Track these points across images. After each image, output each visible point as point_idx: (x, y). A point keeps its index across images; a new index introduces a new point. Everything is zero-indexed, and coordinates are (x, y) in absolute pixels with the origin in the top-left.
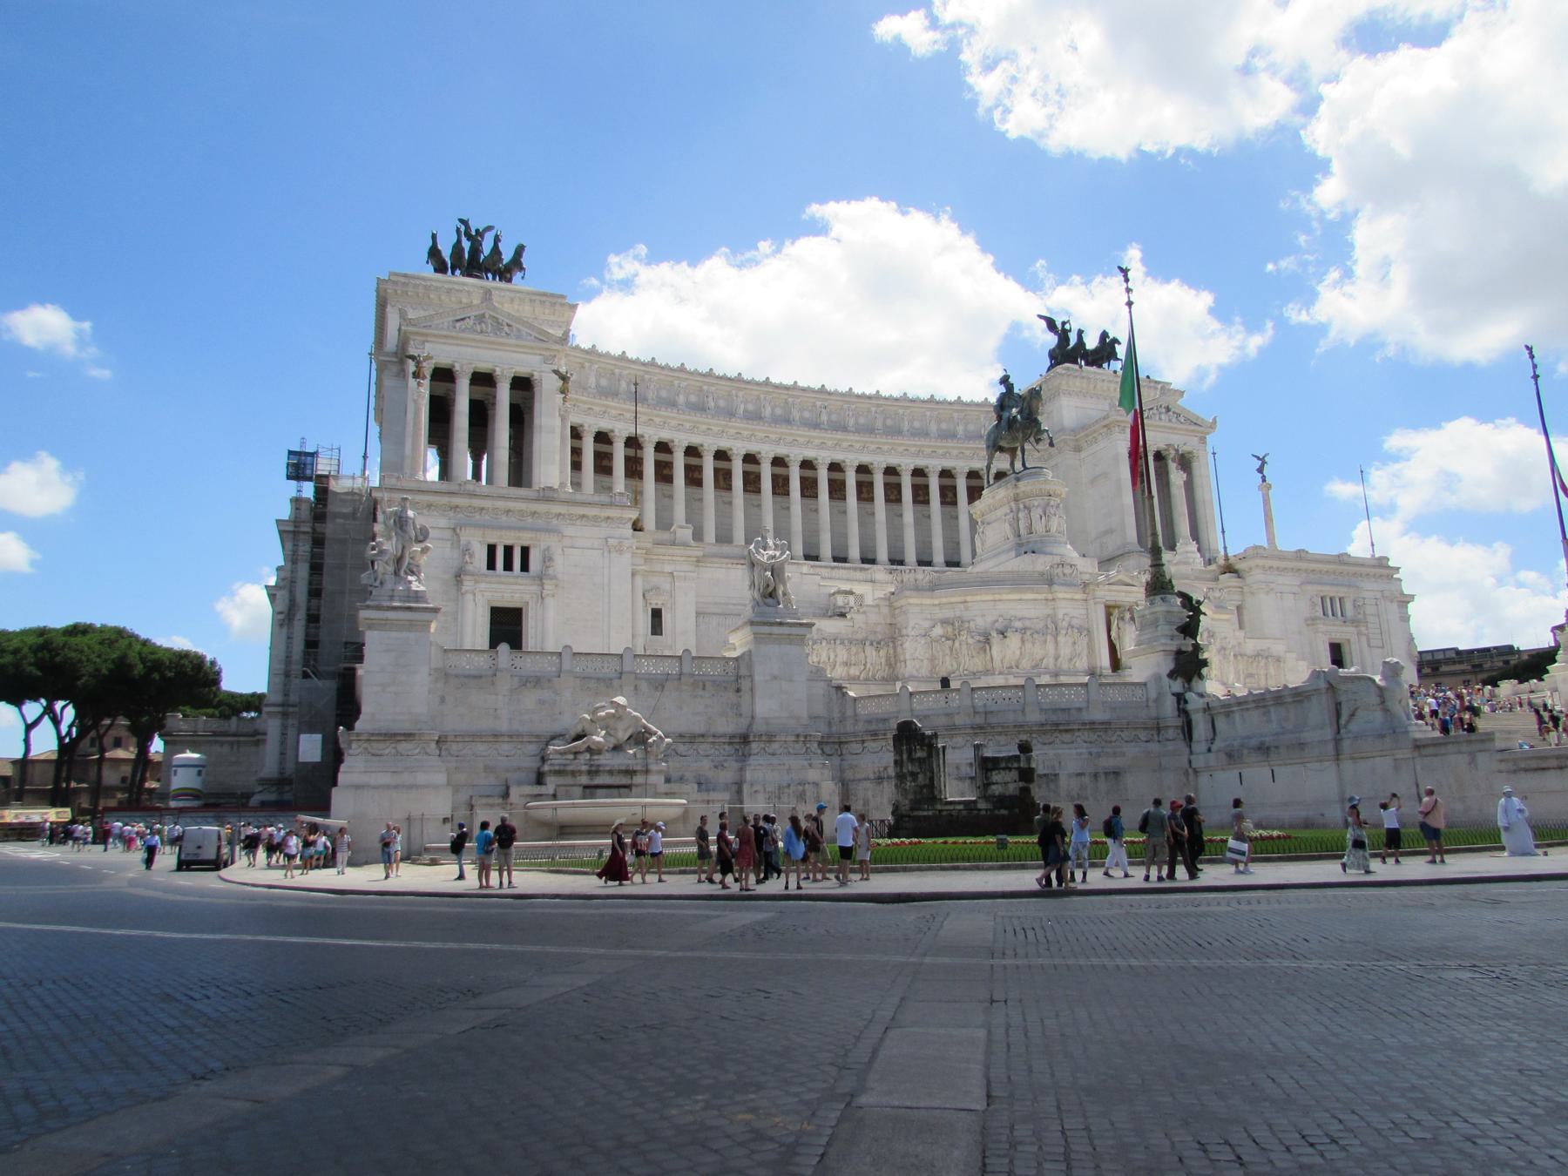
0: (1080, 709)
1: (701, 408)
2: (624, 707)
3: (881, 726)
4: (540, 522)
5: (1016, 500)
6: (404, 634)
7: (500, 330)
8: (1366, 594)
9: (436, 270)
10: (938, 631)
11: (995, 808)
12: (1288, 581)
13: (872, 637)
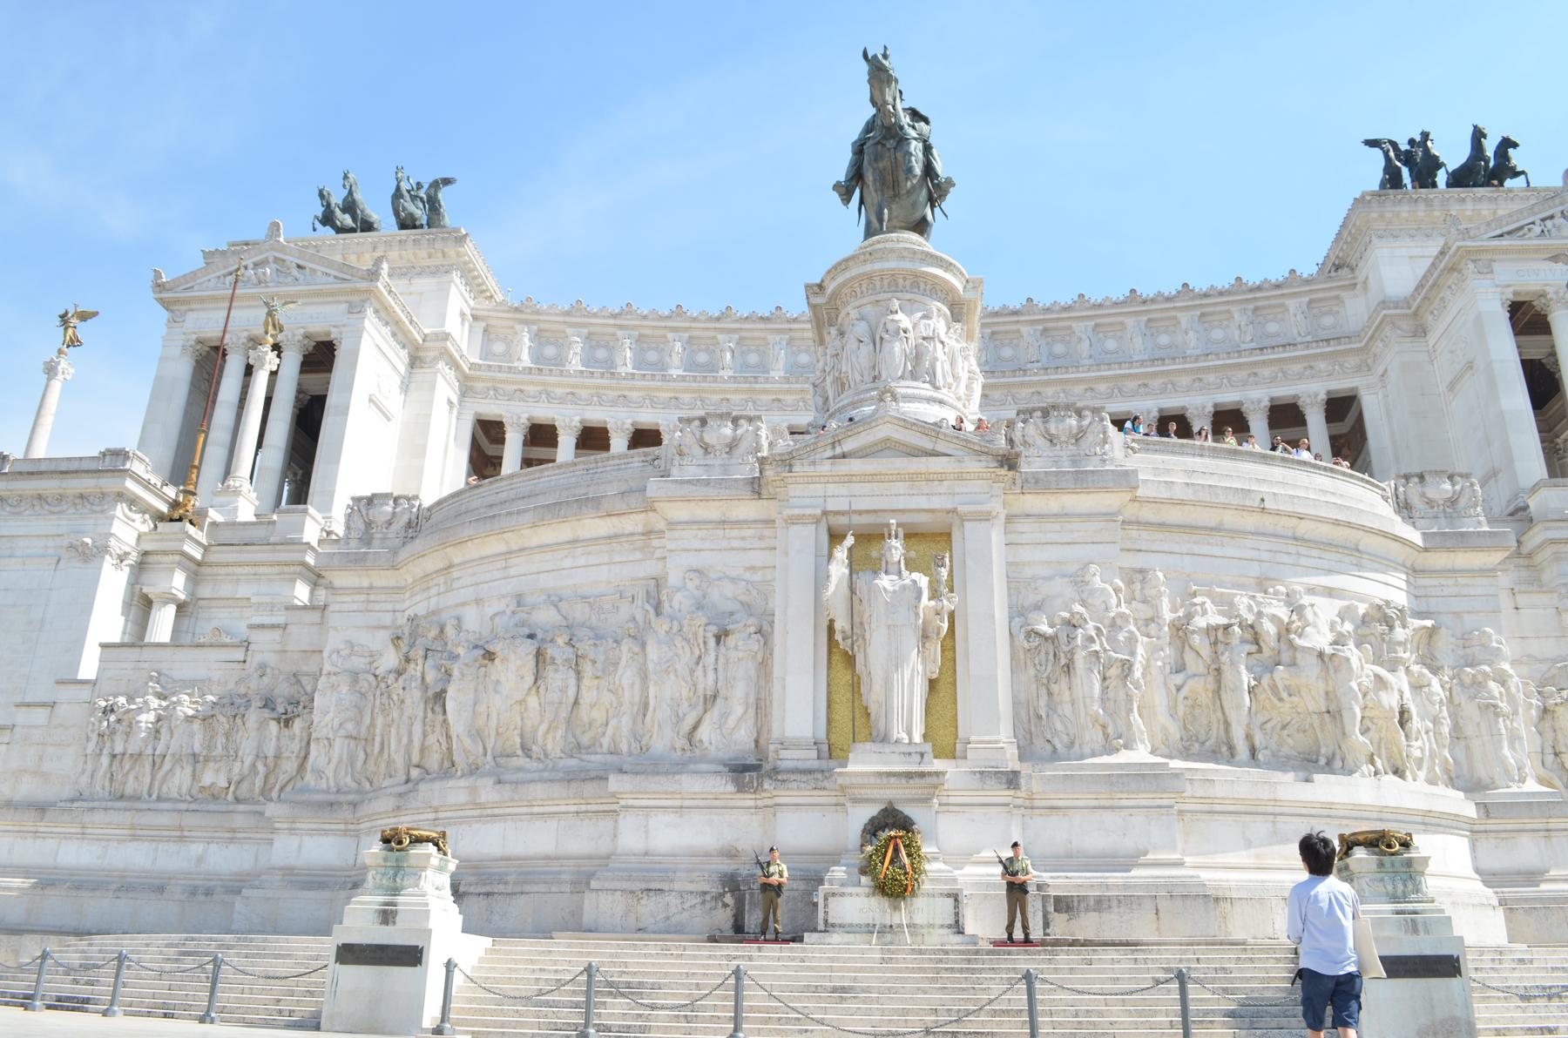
10: (390, 659)
13: (284, 689)
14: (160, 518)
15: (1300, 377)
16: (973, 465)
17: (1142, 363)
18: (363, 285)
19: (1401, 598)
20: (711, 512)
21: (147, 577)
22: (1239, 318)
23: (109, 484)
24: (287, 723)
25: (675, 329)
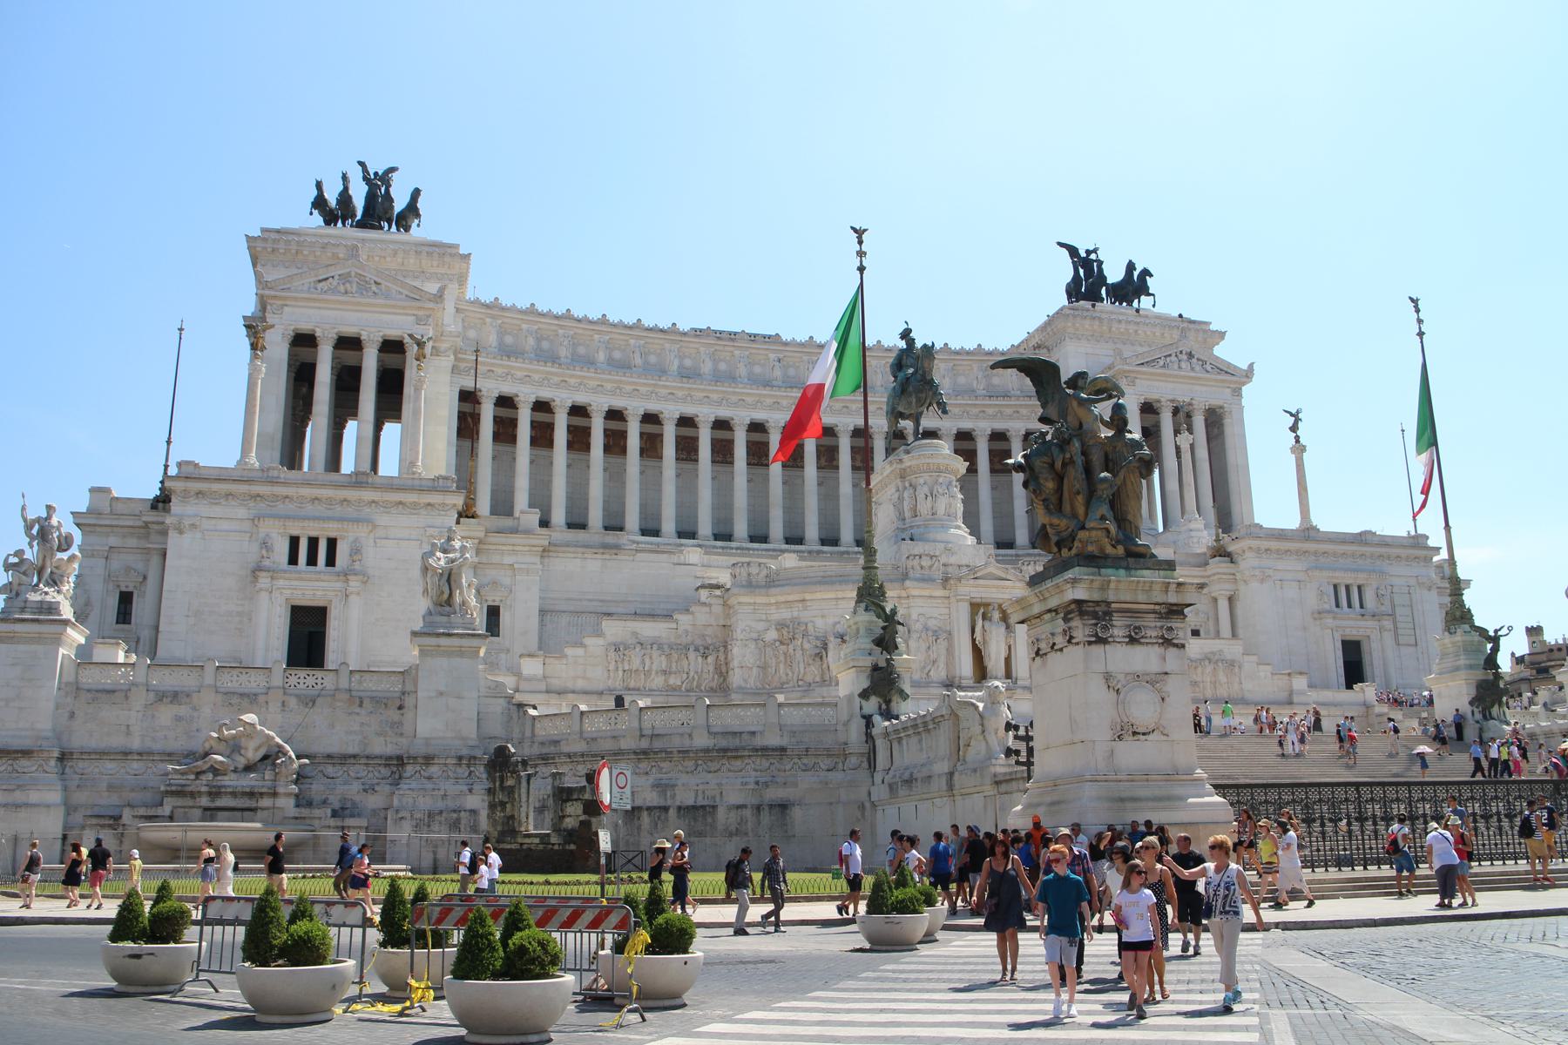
1: (624, 366)
2: (253, 725)
3: (552, 749)
4: (350, 511)
5: (903, 477)
6: (33, 647)
8: (1396, 581)
9: (327, 223)
10: (772, 635)
11: (567, 842)
12: (1292, 566)
13: (699, 642)
14: (460, 515)
15: (1010, 417)
16: (1019, 584)
18: (431, 305)
25: (599, 332)
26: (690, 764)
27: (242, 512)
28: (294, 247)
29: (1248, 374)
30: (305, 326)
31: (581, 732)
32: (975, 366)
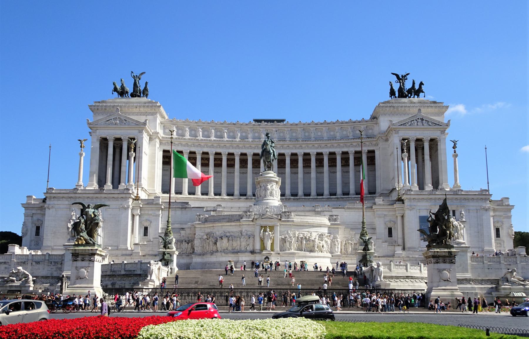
0: (134, 271)
7: (122, 123)
10: (205, 237)
13: (187, 239)
14: (133, 199)
17: (326, 140)
19: (327, 232)
20: (248, 223)
21: (133, 211)
22: (350, 130)
23: (128, 196)
24: (188, 243)
25: (212, 126)
26: (120, 279)
27: (67, 202)
28: (104, 108)
29: (448, 125)
30: (104, 136)
31: (125, 269)
32: (349, 127)
